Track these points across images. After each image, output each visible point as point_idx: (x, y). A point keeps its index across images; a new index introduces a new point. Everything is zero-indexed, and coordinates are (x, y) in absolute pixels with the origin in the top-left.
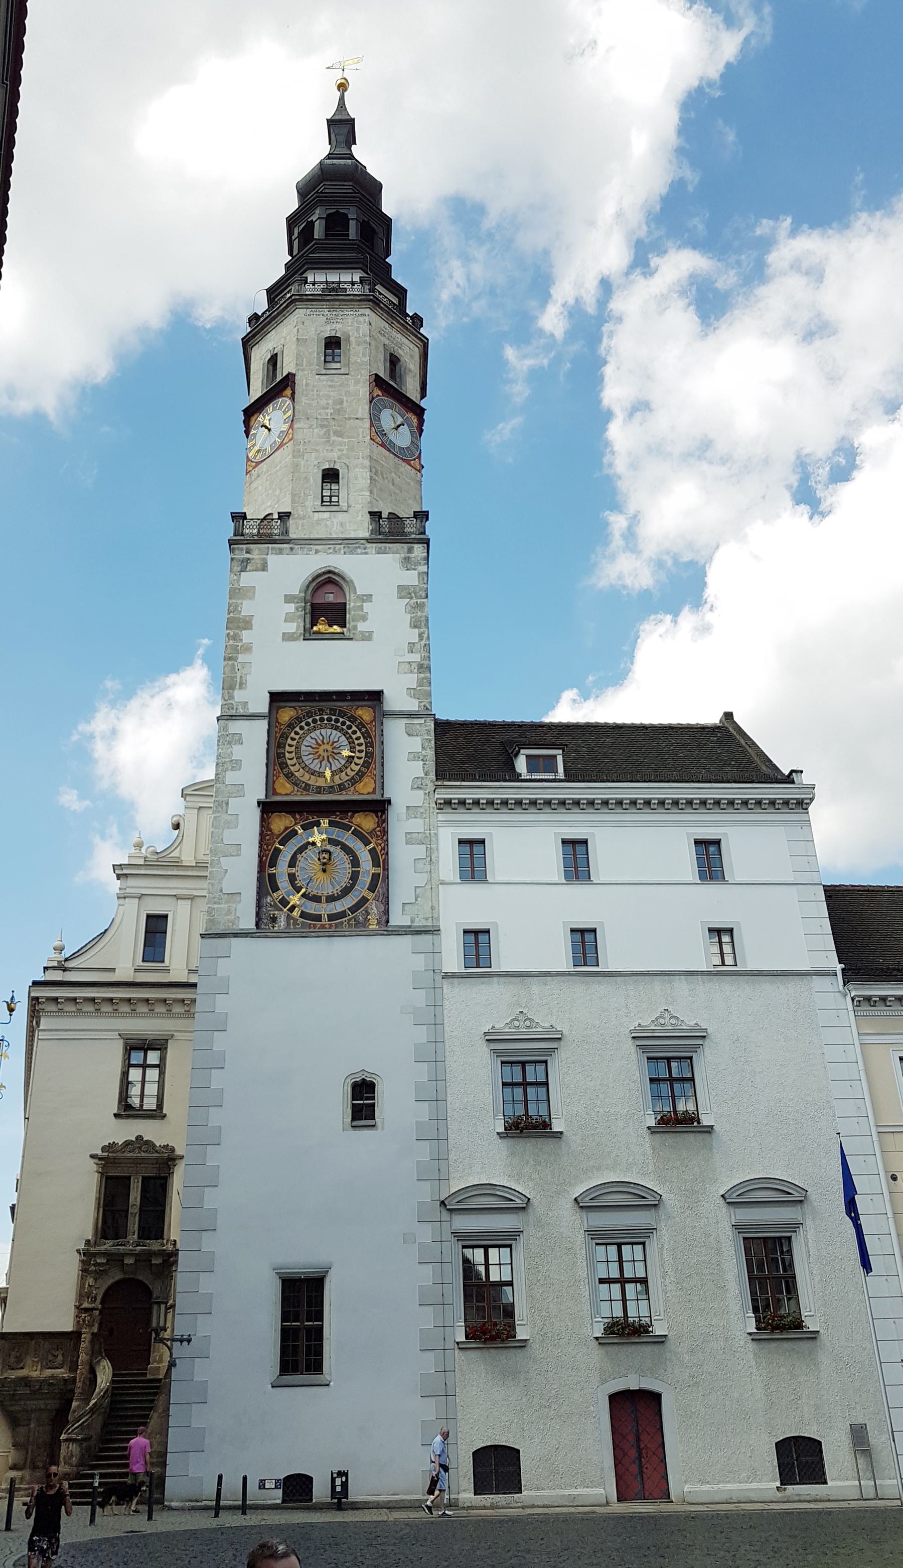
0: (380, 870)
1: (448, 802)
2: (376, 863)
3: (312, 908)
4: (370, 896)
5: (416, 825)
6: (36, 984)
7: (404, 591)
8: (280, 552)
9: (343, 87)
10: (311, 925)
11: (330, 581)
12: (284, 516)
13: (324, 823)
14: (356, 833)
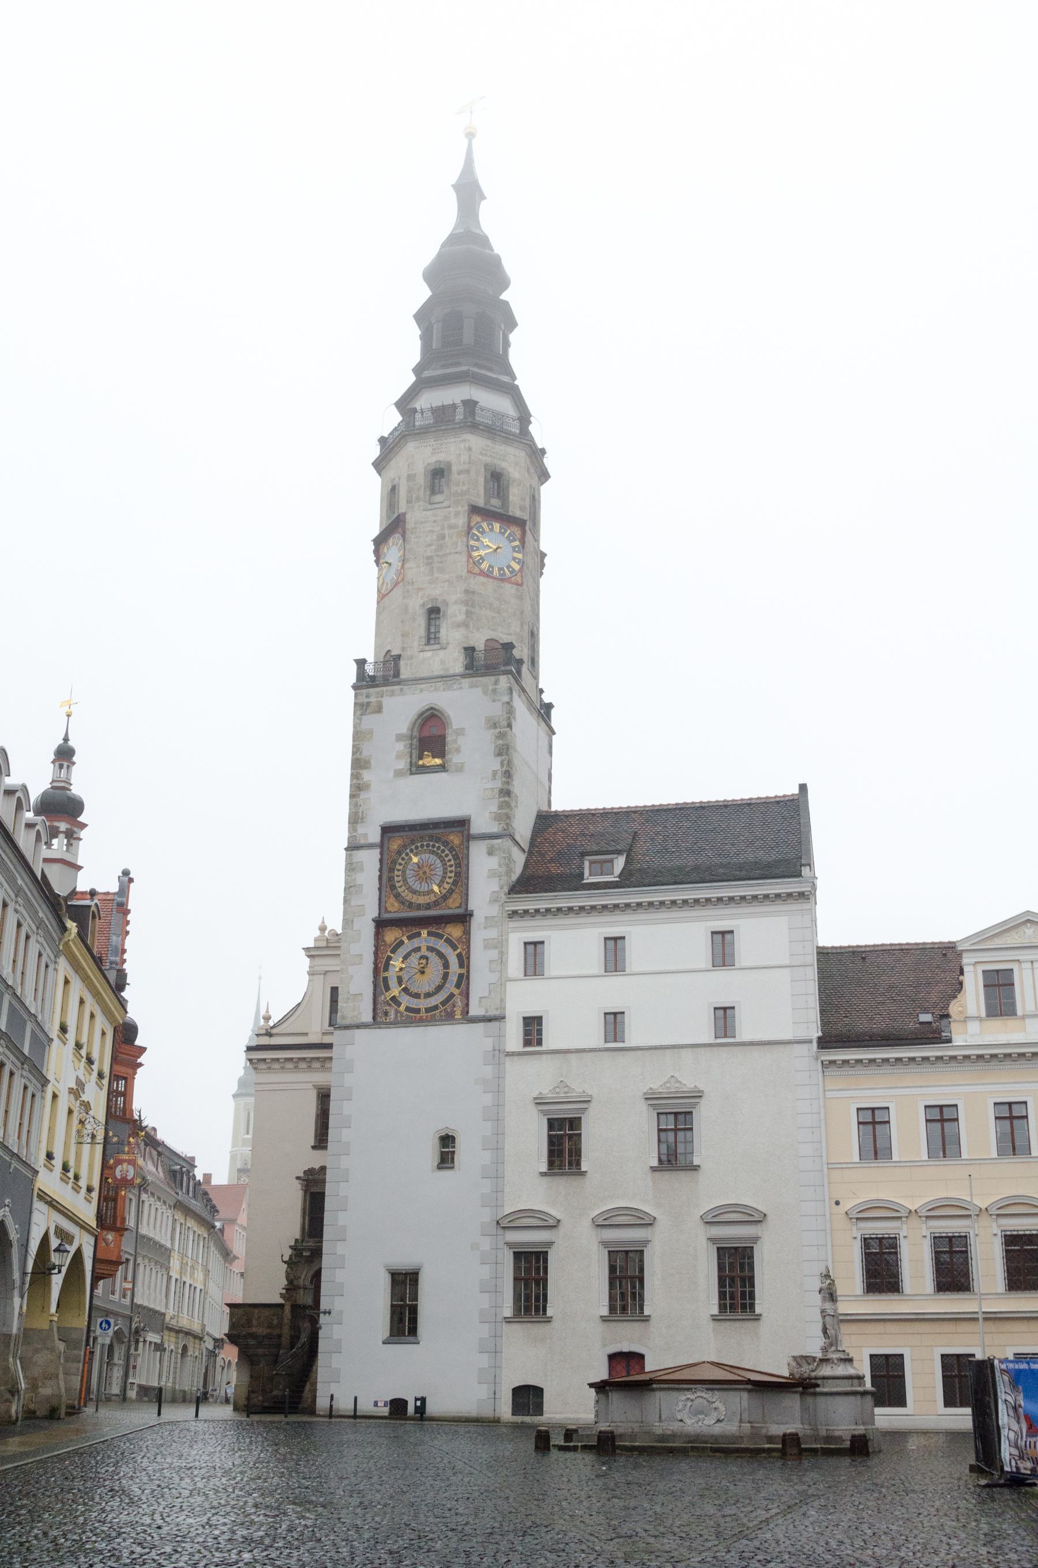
0: (463, 971)
1: (515, 912)
2: (461, 966)
3: (414, 1003)
4: (456, 992)
5: (493, 933)
6: (249, 1049)
8: (392, 694)
9: (470, 135)
10: (414, 1018)
11: (433, 716)
12: (399, 657)
13: (424, 933)
14: (448, 941)
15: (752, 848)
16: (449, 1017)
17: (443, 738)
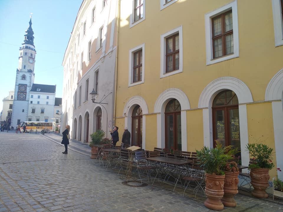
7: (30, 77)
10: (21, 100)
15: (51, 89)
16: (24, 100)
17: (25, 77)
